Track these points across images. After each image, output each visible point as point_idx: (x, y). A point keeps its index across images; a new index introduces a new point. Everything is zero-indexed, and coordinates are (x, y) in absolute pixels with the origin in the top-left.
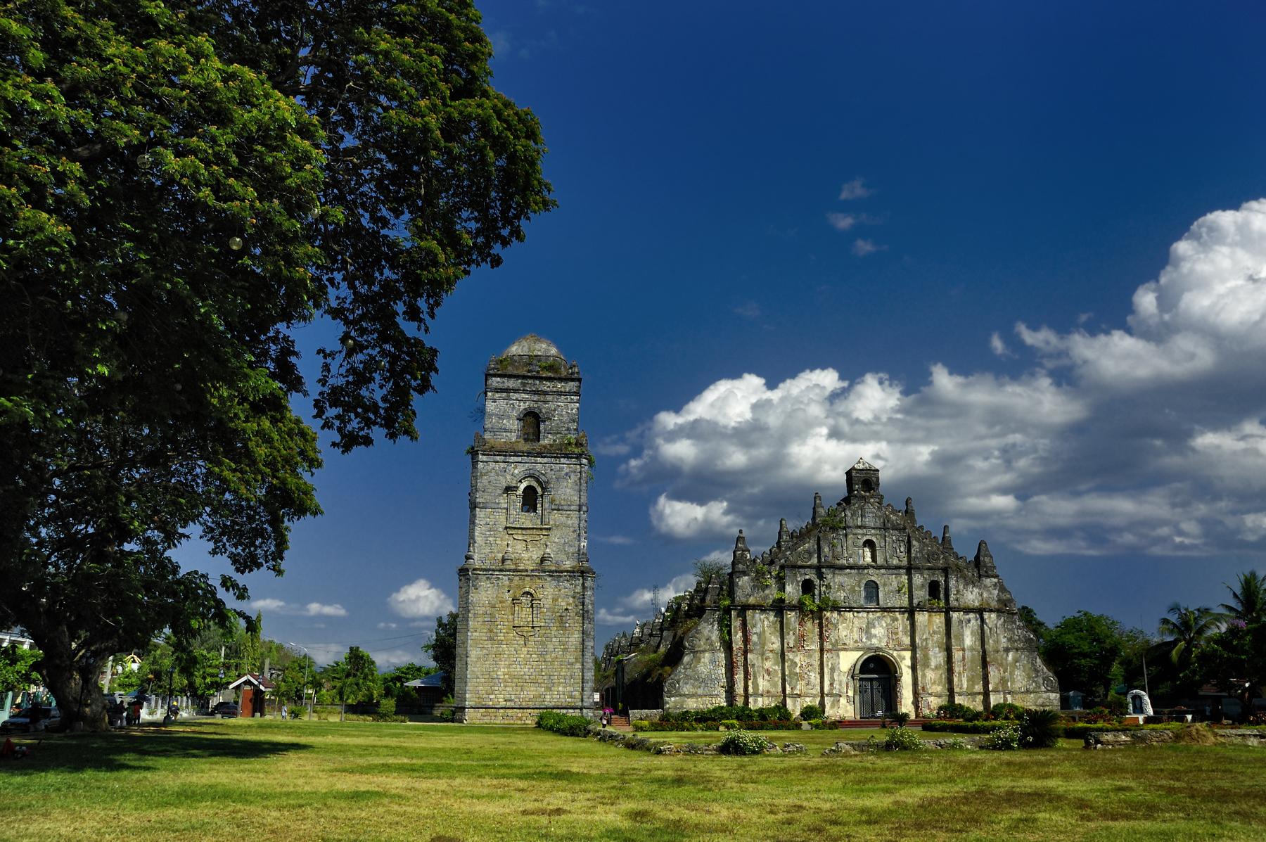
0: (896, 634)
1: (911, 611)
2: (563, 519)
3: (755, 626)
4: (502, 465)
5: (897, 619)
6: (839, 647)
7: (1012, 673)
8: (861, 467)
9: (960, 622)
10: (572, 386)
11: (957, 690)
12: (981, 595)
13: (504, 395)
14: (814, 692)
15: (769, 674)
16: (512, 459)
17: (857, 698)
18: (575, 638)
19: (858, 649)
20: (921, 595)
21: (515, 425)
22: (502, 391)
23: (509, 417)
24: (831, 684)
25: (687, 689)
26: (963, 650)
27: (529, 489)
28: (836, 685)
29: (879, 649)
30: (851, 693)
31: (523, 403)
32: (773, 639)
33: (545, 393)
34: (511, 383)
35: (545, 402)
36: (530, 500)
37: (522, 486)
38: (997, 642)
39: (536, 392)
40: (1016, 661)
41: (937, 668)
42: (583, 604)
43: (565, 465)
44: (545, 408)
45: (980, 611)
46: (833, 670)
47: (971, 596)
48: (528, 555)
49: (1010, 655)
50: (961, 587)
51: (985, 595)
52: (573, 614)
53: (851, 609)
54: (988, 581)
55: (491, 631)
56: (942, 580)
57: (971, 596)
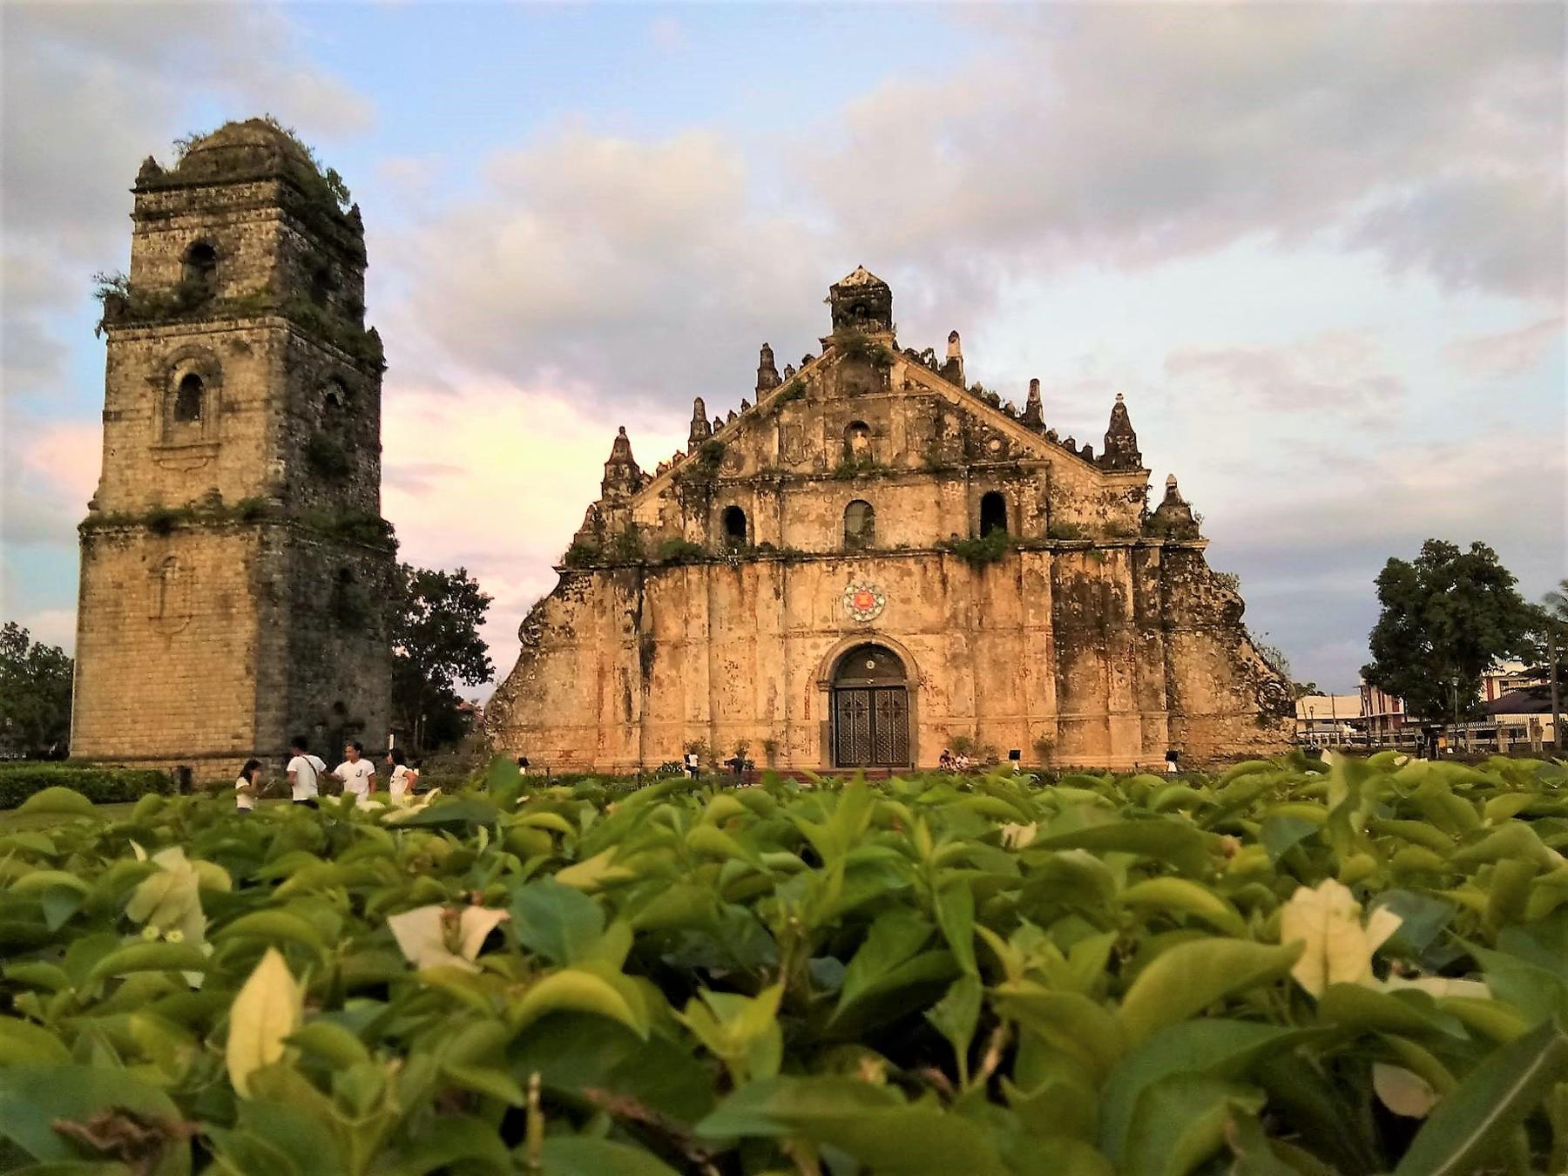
4: (145, 343)
5: (910, 574)
8: (854, 281)
10: (269, 189)
13: (161, 224)
15: (660, 685)
16: (162, 330)
18: (244, 630)
20: (960, 523)
21: (173, 273)
23: (167, 261)
24: (771, 701)
25: (522, 719)
27: (191, 382)
28: (780, 702)
31: (188, 230)
33: (225, 209)
34: (169, 201)
35: (226, 225)
37: (178, 377)
39: (209, 211)
42: (259, 571)
52: (244, 591)
55: (115, 628)
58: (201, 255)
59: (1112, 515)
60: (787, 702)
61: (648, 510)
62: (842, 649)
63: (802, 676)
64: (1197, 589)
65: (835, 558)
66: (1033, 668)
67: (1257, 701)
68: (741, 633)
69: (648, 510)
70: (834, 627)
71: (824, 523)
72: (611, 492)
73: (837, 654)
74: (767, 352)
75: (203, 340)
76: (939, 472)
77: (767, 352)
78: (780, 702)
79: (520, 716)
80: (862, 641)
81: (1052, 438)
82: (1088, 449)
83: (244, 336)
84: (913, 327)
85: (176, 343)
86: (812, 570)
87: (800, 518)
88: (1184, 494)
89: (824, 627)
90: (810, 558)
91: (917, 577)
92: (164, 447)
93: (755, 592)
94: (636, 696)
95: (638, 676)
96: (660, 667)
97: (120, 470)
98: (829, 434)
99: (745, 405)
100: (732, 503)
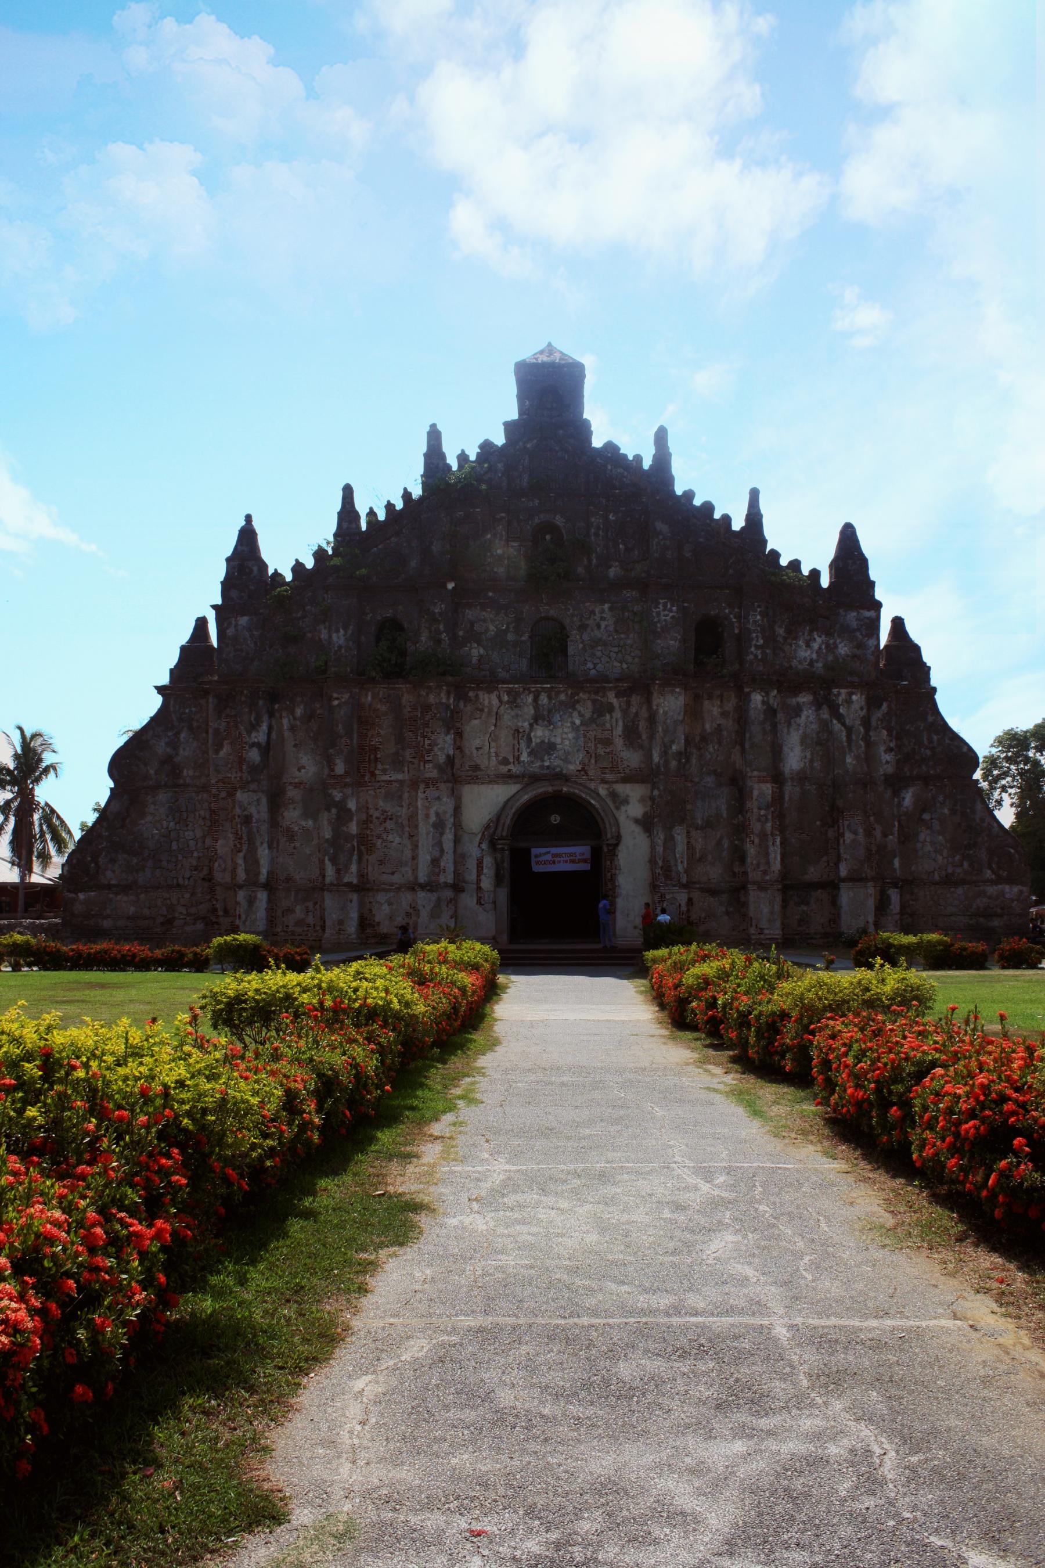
0: (608, 742)
1: (638, 686)
3: (254, 727)
5: (611, 709)
6: (456, 775)
7: (907, 838)
8: (544, 358)
9: (771, 712)
11: (754, 875)
12: (831, 648)
14: (396, 879)
17: (503, 895)
19: (508, 778)
24: (435, 862)
25: (111, 876)
26: (777, 778)
30: (487, 883)
32: (305, 759)
38: (869, 757)
40: (922, 806)
41: (708, 825)
45: (822, 685)
46: (439, 826)
47: (807, 651)
49: (908, 798)
50: (781, 631)
51: (843, 649)
53: (491, 683)
54: (851, 618)
57: (807, 651)
59: (843, 649)
60: (455, 863)
62: (526, 797)
64: (931, 741)
66: (756, 827)
67: (990, 867)
68: (400, 777)
70: (515, 769)
72: (234, 594)
73: (518, 804)
74: (434, 436)
78: (448, 862)
79: (109, 874)
80: (550, 789)
81: (775, 555)
82: (815, 574)
86: (489, 700)
88: (915, 632)
89: (504, 769)
91: (617, 714)
94: (264, 853)
95: (264, 827)
96: (291, 816)
99: (407, 495)
100: (389, 613)
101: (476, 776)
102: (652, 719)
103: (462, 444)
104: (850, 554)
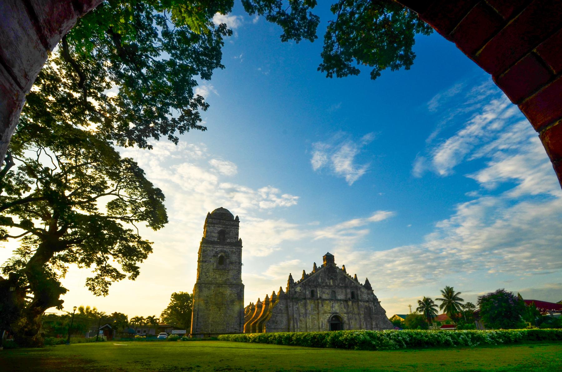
2: (234, 268)
20: (349, 296)
21: (216, 235)
22: (212, 223)
23: (214, 233)
27: (222, 257)
29: (336, 313)
31: (218, 228)
35: (227, 228)
36: (222, 261)
37: (219, 255)
43: (234, 249)
44: (227, 230)
48: (220, 280)
53: (326, 300)
56: (355, 291)
58: (222, 234)
61: (298, 289)
63: (326, 320)
65: (330, 300)
69: (298, 289)
71: (328, 294)
75: (225, 249)
76: (346, 287)
77: (315, 264)
83: (234, 250)
84: (339, 263)
85: (219, 249)
86: (327, 302)
87: (324, 293)
90: (326, 300)
92: (217, 269)
93: (318, 305)
97: (205, 273)
98: (328, 279)
101: (325, 312)
102: (348, 305)
103: (319, 265)
104: (367, 281)
